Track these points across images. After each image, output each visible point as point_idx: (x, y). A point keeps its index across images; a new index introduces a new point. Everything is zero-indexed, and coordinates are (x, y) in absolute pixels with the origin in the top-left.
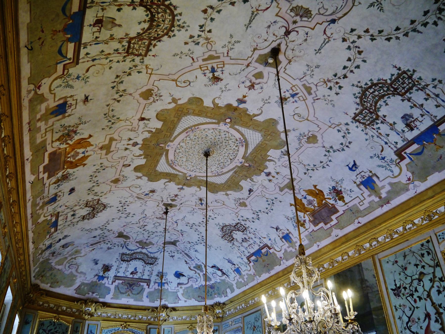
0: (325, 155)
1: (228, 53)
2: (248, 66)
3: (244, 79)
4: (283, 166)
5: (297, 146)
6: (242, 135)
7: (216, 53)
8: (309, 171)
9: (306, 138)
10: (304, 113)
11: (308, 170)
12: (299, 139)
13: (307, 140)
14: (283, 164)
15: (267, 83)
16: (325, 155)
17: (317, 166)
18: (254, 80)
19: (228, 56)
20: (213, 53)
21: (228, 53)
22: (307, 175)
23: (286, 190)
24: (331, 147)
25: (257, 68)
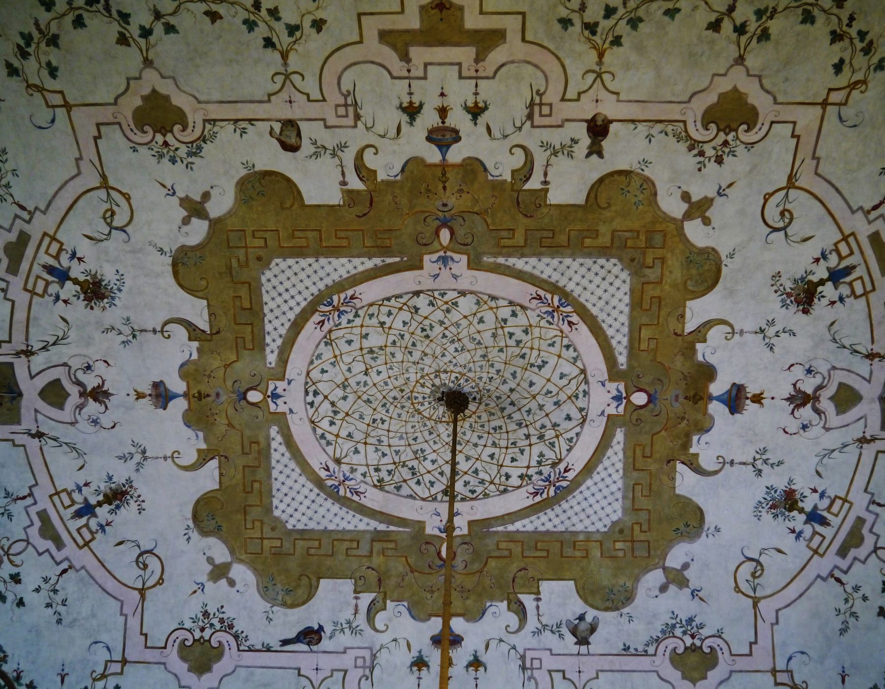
0: (170, 29)
1: (24, 498)
2: (39, 435)
3: (84, 425)
4: (357, 117)
5: (226, 132)
6: (297, 326)
7: (32, 524)
8: (294, 20)
9: (169, 138)
10: (97, 202)
11: (292, 30)
12: (195, 149)
13: (177, 128)
14: (350, 121)
15: (65, 365)
16: (170, 29)
17: (244, 15)
18: (74, 398)
19: (31, 494)
20: (34, 532)
21: (24, 498)
22: (320, 15)
23: (472, 21)
24: (123, 40)
25: (36, 411)
